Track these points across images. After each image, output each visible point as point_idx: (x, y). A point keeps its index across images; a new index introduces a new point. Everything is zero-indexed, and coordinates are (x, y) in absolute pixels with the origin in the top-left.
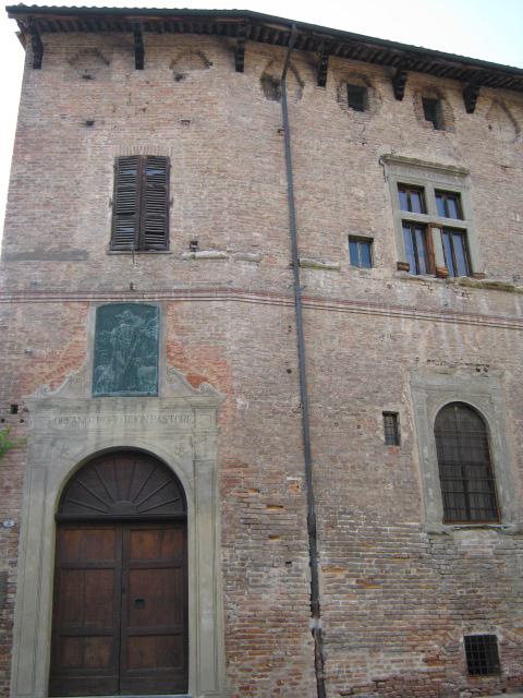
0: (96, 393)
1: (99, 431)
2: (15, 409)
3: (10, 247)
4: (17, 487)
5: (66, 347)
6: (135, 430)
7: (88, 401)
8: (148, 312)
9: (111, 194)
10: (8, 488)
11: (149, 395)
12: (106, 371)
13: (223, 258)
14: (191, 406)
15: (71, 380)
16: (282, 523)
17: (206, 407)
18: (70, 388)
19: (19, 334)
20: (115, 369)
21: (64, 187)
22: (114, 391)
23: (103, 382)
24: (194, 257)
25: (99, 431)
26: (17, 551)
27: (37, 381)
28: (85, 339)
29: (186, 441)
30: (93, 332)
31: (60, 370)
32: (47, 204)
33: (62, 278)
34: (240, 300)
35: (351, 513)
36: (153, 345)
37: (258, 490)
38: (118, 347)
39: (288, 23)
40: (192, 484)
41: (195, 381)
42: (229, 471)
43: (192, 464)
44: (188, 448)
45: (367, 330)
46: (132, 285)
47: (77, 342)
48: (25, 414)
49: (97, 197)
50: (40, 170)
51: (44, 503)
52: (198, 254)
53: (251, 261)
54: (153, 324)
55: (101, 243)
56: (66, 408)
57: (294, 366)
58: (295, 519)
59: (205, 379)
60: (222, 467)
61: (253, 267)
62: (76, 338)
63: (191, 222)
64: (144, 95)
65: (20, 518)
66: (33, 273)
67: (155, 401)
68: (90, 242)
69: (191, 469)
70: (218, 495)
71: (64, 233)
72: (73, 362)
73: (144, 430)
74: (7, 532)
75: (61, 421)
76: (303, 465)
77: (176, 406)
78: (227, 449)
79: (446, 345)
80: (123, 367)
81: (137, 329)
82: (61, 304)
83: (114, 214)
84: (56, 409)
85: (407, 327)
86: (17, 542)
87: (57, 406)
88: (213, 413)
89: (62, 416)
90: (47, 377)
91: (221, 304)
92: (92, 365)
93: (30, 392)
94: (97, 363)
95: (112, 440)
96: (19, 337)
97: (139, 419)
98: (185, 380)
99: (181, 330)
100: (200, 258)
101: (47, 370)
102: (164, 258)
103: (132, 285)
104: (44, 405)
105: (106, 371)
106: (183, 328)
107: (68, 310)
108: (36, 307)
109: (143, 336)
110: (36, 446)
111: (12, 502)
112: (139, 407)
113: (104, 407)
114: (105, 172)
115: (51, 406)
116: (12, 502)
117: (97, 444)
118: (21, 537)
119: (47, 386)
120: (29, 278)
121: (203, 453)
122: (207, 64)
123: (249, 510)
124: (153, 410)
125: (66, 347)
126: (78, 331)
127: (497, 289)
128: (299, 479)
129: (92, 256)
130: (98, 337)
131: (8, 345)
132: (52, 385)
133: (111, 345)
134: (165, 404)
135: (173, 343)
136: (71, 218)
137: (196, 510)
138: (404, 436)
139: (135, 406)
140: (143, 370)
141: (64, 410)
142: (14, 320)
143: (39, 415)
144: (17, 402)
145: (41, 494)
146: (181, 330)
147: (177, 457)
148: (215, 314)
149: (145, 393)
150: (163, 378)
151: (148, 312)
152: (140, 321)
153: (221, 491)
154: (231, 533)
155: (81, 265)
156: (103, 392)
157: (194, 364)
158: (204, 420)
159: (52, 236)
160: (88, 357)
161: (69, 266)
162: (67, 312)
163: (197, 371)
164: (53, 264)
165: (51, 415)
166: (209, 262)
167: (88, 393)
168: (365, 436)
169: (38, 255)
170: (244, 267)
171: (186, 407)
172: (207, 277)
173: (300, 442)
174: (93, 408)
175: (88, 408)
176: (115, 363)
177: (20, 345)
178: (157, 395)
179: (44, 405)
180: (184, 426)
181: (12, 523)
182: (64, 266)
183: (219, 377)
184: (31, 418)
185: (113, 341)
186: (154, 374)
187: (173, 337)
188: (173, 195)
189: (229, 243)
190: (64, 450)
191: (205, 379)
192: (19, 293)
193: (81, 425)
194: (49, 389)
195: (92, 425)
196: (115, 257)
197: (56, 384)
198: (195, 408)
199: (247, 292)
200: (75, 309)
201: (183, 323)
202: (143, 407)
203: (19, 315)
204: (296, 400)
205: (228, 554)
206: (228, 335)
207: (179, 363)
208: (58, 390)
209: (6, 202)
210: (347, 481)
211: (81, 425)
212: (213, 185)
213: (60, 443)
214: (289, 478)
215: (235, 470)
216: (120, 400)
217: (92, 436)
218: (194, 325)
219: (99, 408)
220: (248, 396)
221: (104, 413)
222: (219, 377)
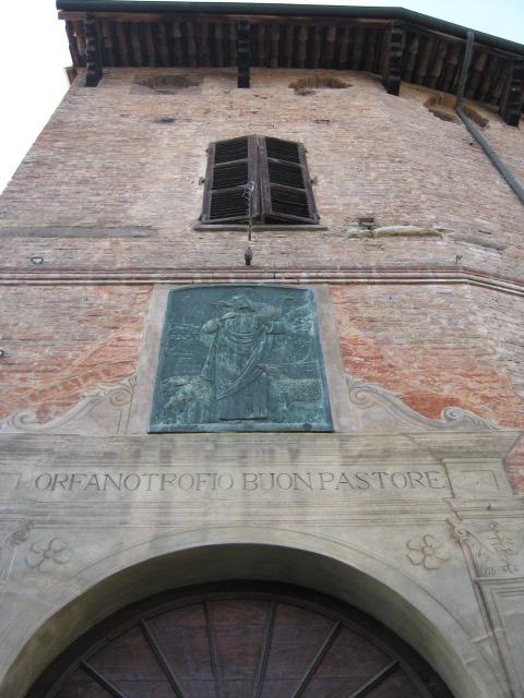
0: (161, 426)
1: (164, 507)
8: (291, 295)
11: (307, 429)
12: (188, 385)
14: (430, 452)
17: (469, 453)
18: (90, 414)
22: (210, 421)
23: (181, 407)
25: (164, 507)
29: (437, 532)
30: (160, 324)
34: (489, 286)
36: (307, 346)
40: (489, 649)
43: (469, 590)
44: (448, 549)
46: (248, 259)
47: (119, 339)
52: (377, 230)
53: (487, 246)
56: (74, 455)
59: (453, 402)
61: (493, 254)
69: (472, 605)
71: (109, 209)
73: (301, 504)
75: (52, 485)
77: (387, 454)
80: (234, 378)
81: (262, 321)
84: (44, 457)
87: (49, 452)
88: (496, 466)
89: (60, 471)
90: (33, 397)
91: (448, 289)
92: (153, 376)
94: (166, 369)
95: (205, 528)
97: (285, 481)
98: (400, 402)
101: (35, 383)
102: (311, 235)
103: (248, 259)
106: (371, 320)
107: (106, 296)
109: (280, 333)
112: (282, 454)
115: (30, 451)
121: (496, 561)
124: (323, 463)
134: (356, 448)
135: (355, 342)
139: (272, 452)
140: (285, 385)
141: (64, 459)
147: (419, 573)
151: (291, 295)
155: (142, 242)
157: (415, 375)
163: (425, 388)
166: (404, 241)
167: (141, 425)
171: (414, 453)
175: (137, 454)
180: (422, 494)
182: (106, 243)
187: (352, 332)
191: (453, 402)
193: (111, 490)
194: (33, 417)
197: (54, 408)
198: (440, 455)
202: (295, 454)
207: (374, 373)
209: (10, 179)
211: (111, 490)
213: (40, 537)
216: (226, 439)
219: (166, 457)
221: (179, 467)
222: (485, 398)
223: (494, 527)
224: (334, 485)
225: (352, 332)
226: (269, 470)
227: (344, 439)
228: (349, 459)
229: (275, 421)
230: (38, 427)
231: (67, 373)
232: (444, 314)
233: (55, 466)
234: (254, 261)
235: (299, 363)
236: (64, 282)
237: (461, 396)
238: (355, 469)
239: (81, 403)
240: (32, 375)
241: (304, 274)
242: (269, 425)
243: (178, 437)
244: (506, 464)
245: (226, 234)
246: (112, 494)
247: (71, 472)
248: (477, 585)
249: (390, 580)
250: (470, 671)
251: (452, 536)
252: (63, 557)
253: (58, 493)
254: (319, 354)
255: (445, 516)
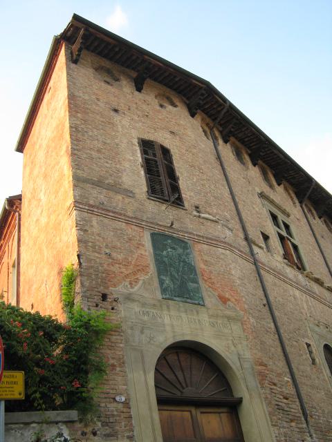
1: (172, 326)
2: (104, 297)
3: (78, 171)
4: (120, 366)
5: (135, 256)
6: (197, 329)
7: (159, 301)
9: (140, 160)
10: (113, 366)
11: (199, 304)
13: (217, 222)
15: (144, 283)
16: (293, 410)
18: (144, 287)
19: (97, 238)
20: (172, 280)
21: (108, 144)
22: (175, 296)
24: (199, 217)
26: (132, 424)
27: (118, 278)
28: (147, 254)
29: (230, 342)
30: (152, 251)
31: (134, 273)
32: (99, 151)
33: (120, 205)
35: (315, 408)
36: (192, 269)
37: (275, 384)
38: (171, 265)
39: (225, 100)
41: (224, 300)
42: (260, 367)
44: (233, 348)
45: (285, 291)
46: (172, 224)
47: (142, 254)
48: (114, 304)
49: (132, 158)
50: (90, 127)
51: (146, 380)
52: (203, 215)
54: (188, 254)
55: (141, 189)
56: (146, 304)
57: (265, 302)
58: (295, 408)
59: (229, 300)
60: (256, 365)
62: (139, 252)
63: (192, 194)
64: (144, 107)
65: (128, 395)
66: (97, 196)
67: (203, 309)
68: (134, 186)
69: (239, 364)
70: (259, 386)
72: (143, 269)
74: (120, 406)
76: (288, 370)
78: (254, 351)
79: (312, 309)
82: (124, 224)
83: (145, 172)
85: (297, 293)
86: (130, 417)
88: (240, 325)
91: (224, 251)
92: (156, 274)
93: (115, 286)
94: (159, 274)
95: (183, 335)
96: (98, 240)
99: (206, 262)
100: (204, 218)
103: (172, 224)
104: (129, 298)
105: (167, 281)
106: (206, 261)
108: (106, 221)
109: (184, 261)
110: (129, 331)
111: (119, 379)
113: (171, 308)
114: (133, 144)
115: (133, 301)
116: (119, 379)
117: (174, 336)
118: (133, 412)
119: (127, 283)
120: (97, 198)
122: (176, 106)
123: (277, 399)
124: (204, 317)
125: (135, 256)
126: (141, 247)
127: (319, 283)
128: (287, 379)
129: (137, 196)
130: (155, 255)
131: (90, 244)
132: (131, 284)
133: (164, 262)
136: (118, 166)
137: (250, 395)
138: (317, 360)
139: (192, 311)
140: (191, 285)
141: (144, 305)
142: (92, 226)
143: (126, 305)
144: (106, 291)
145: (142, 372)
146: (206, 262)
147: (227, 353)
148: (222, 257)
149: (196, 302)
150: (205, 294)
152: (180, 251)
153: (260, 383)
154: (274, 416)
156: (168, 296)
158: (236, 328)
159: (108, 174)
160: (152, 268)
161: (123, 198)
162: (131, 231)
164: (111, 194)
165: (136, 308)
166: (209, 223)
167: (159, 295)
168: (304, 357)
169: (99, 184)
170: (228, 233)
172: (210, 231)
173: (282, 354)
174: (164, 307)
175: (161, 306)
176: (171, 274)
177: (100, 247)
178: (204, 306)
179: (129, 298)
180: (226, 331)
181: (123, 399)
182: (120, 197)
183: (236, 300)
184: (120, 307)
185: (166, 259)
186: (198, 290)
187: (202, 266)
188: (178, 174)
189: (217, 214)
190: (151, 338)
192: (93, 206)
195: (167, 321)
196: (152, 202)
197: (133, 283)
198: (229, 318)
199: (234, 247)
200: (134, 230)
201: (206, 258)
202: (198, 313)
203: (94, 223)
204: (272, 325)
205: (277, 432)
206: (233, 272)
208: (136, 288)
210: (307, 385)
212: (198, 175)
213: (147, 332)
214: (286, 379)
215: (264, 368)
216: (181, 304)
217: (168, 328)
218: (213, 261)
219: (168, 307)
220: (253, 317)
221: (172, 313)
222: (236, 300)
223: (241, 343)
224: (207, 325)
225: (202, 266)
226: (193, 317)
227: (208, 309)
228: (211, 316)
229: (191, 299)
230: (131, 290)
231: (131, 267)
232: (224, 263)
233: (142, 307)
234: (174, 226)
235: (192, 276)
236: (114, 219)
237: (230, 297)
238: (211, 320)
239: (141, 282)
240: (121, 266)
241: (186, 235)
242: (189, 300)
243: (170, 301)
244: (242, 324)
245: (157, 203)
246: (159, 320)
247: (147, 310)
248: (239, 358)
249: (223, 355)
250: (240, 380)
251: (234, 345)
252: (155, 340)
253: (146, 318)
254: (196, 274)
255: (231, 338)
